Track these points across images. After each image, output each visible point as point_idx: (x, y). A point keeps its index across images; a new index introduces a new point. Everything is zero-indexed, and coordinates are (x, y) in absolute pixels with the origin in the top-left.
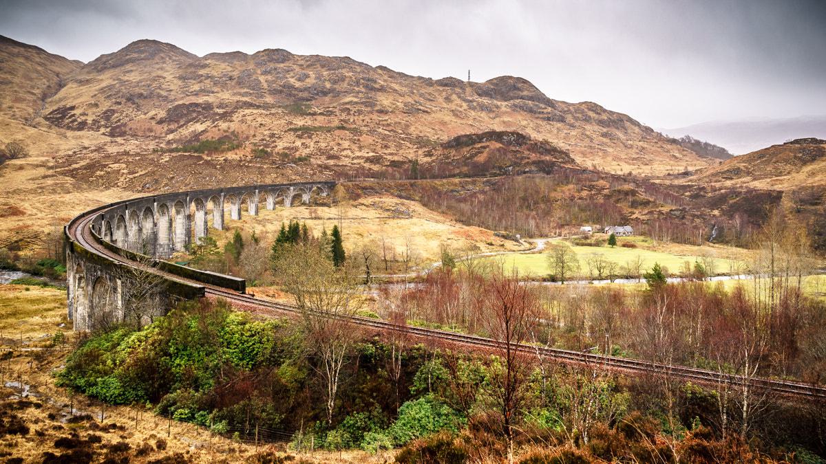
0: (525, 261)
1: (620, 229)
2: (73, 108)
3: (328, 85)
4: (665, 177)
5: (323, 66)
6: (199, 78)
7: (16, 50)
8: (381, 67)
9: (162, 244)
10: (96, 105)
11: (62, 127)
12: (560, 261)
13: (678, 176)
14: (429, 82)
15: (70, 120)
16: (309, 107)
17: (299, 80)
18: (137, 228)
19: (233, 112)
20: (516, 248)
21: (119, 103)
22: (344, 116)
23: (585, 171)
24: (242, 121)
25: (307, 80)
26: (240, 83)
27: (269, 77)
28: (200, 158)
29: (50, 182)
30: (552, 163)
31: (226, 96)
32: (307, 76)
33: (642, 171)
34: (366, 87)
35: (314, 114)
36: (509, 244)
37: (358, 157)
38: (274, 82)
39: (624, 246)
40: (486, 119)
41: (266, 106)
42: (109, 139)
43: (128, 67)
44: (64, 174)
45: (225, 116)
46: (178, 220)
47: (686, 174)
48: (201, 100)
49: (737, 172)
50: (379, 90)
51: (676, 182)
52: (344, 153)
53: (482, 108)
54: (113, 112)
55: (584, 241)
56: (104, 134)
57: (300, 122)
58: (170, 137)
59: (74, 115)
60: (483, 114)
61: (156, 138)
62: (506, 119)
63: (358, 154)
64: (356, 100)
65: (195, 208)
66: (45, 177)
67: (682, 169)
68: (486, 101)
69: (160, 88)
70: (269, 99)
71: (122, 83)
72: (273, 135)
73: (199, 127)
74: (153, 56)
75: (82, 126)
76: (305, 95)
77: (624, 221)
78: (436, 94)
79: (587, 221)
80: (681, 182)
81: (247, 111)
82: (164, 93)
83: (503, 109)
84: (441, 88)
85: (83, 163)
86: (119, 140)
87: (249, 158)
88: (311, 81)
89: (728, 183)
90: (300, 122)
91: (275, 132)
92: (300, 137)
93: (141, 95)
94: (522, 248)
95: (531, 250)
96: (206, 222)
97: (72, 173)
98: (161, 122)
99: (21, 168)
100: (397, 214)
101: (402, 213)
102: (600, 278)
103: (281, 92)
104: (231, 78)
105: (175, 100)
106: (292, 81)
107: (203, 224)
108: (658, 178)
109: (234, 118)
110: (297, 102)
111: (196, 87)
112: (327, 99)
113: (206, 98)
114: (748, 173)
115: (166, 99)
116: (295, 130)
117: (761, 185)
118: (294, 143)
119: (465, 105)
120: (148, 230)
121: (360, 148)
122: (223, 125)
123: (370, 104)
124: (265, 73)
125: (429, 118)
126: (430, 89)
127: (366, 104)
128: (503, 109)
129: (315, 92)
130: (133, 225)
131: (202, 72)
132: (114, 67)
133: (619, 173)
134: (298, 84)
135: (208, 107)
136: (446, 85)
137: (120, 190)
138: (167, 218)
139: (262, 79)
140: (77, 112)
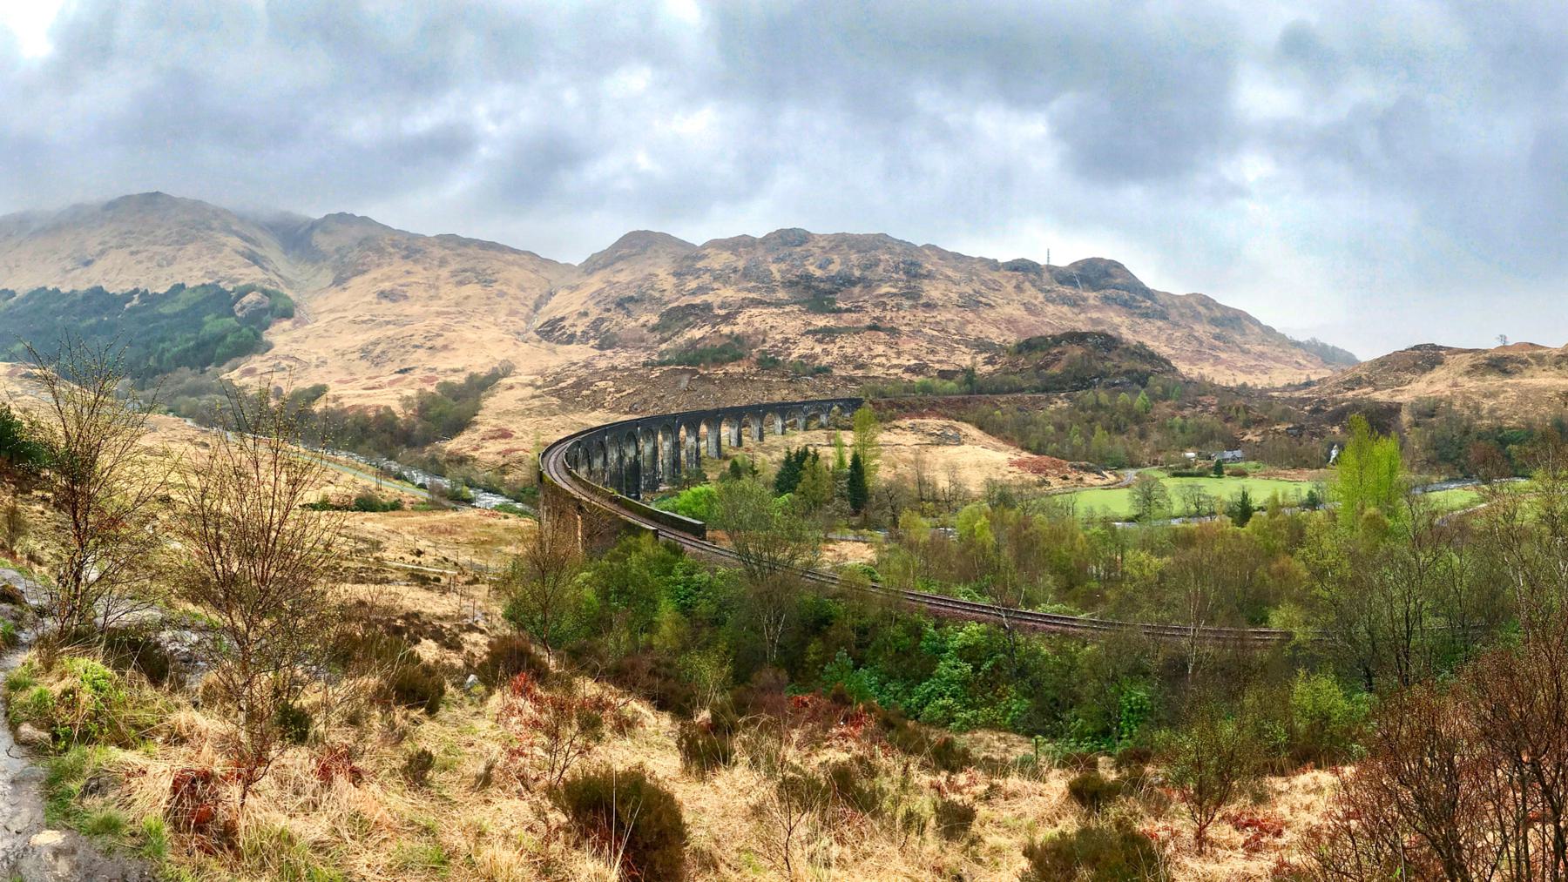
0: (1103, 499)
1: (1229, 455)
2: (563, 319)
3: (857, 273)
4: (1284, 389)
5: (851, 247)
6: (697, 274)
7: (511, 257)
8: (929, 247)
10: (586, 314)
12: (1148, 498)
13: (1298, 388)
14: (994, 265)
16: (833, 302)
17: (820, 267)
19: (738, 313)
20: (1099, 482)
21: (608, 310)
22: (877, 313)
23: (1190, 382)
24: (748, 324)
25: (831, 267)
26: (746, 275)
27: (783, 266)
28: (695, 372)
29: (537, 402)
30: (1145, 369)
31: (729, 293)
32: (831, 262)
33: (1258, 381)
34: (907, 273)
35: (839, 311)
36: (1089, 478)
37: (895, 366)
38: (788, 271)
39: (1231, 474)
40: (1070, 315)
41: (779, 304)
42: (597, 352)
43: (619, 266)
44: (550, 394)
45: (727, 319)
47: (1308, 384)
48: (698, 300)
49: (1357, 382)
50: (925, 277)
51: (1297, 394)
52: (877, 361)
53: (1065, 300)
54: (603, 320)
55: (1183, 471)
57: (820, 322)
58: (664, 346)
60: (1065, 309)
61: (647, 349)
62: (1095, 315)
63: (895, 362)
64: (894, 290)
66: (534, 397)
67: (1303, 379)
68: (1068, 291)
69: (652, 288)
70: (782, 294)
71: (611, 284)
72: (786, 340)
73: (697, 334)
74: (644, 249)
75: (571, 339)
76: (827, 286)
77: (1233, 444)
78: (1003, 282)
79: (1189, 446)
80: (1303, 394)
81: (755, 311)
82: (657, 295)
83: (1091, 302)
84: (1009, 274)
85: (570, 381)
86: (609, 353)
87: (754, 370)
88: (835, 268)
89: (1350, 394)
90: (820, 322)
92: (820, 341)
93: (631, 299)
94: (1106, 482)
95: (1115, 485)
97: (558, 393)
98: (654, 329)
99: (511, 387)
100: (942, 439)
101: (948, 437)
102: (1198, 514)
103: (797, 283)
104: (735, 271)
105: (669, 302)
106: (811, 269)
108: (1276, 390)
109: (739, 320)
110: (816, 295)
111: (692, 284)
112: (857, 290)
113: (704, 297)
114: (1370, 383)
115: (658, 301)
116: (815, 332)
117: (1382, 396)
119: (1041, 296)
121: (899, 354)
122: (726, 330)
123: (913, 295)
124: (778, 260)
125: (993, 314)
126: (996, 275)
127: (908, 296)
128: (1091, 302)
131: (700, 265)
132: (605, 267)
133: (1232, 384)
134: (818, 273)
135: (707, 307)
136: (1016, 269)
139: (774, 268)
140: (566, 323)
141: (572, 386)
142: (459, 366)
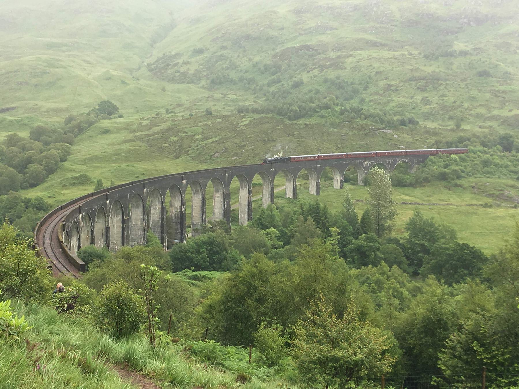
2: (178, 55)
11: (163, 79)
15: (172, 70)
18: (160, 207)
37: (494, 118)
42: (207, 94)
46: (216, 199)
56: (203, 87)
63: (496, 112)
65: (212, 189)
91: (393, 83)
96: (249, 202)
99: (106, 131)
107: (247, 204)
118: (412, 97)
120: (177, 208)
129: (465, 20)
130: (157, 203)
137: (189, 159)
138: (201, 197)
141: (163, 132)
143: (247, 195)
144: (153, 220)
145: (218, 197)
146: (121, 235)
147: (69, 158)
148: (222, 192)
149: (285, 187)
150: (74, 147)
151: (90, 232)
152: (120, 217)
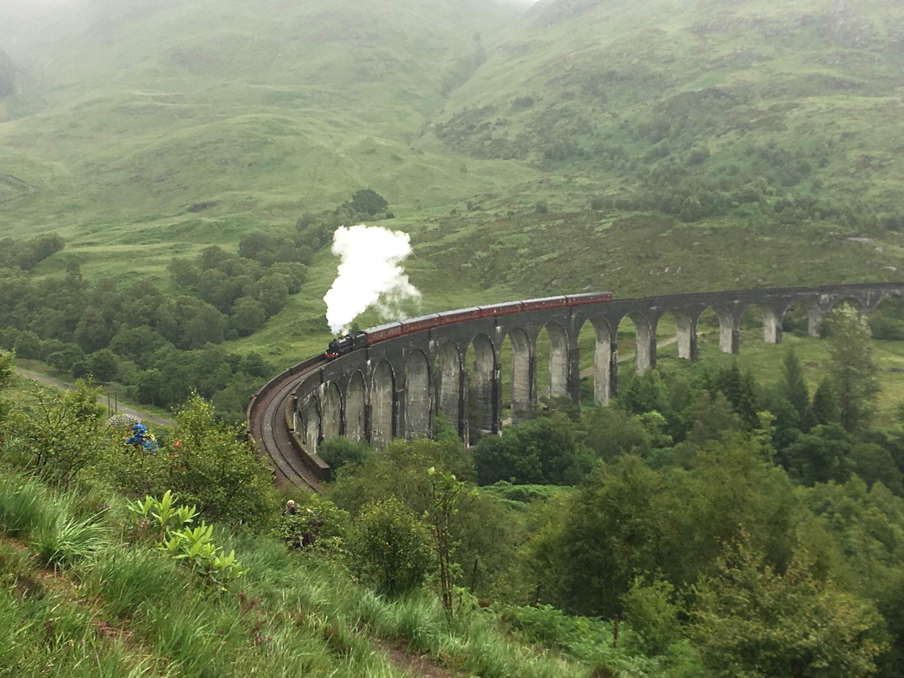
9: (518, 401)
11: (464, 152)
15: (480, 136)
42: (537, 176)
46: (555, 359)
56: (531, 165)
59: (486, 126)
65: (548, 342)
72: (865, 162)
91: (875, 153)
96: (612, 365)
107: (608, 367)
120: (485, 374)
137: (508, 289)
138: (527, 355)
141: (461, 242)
142: (295, 198)
143: (609, 352)
144: (446, 395)
145: (558, 356)
146: (389, 419)
147: (303, 287)
148: (564, 348)
149: (673, 340)
150: (313, 270)
151: (338, 415)
152: (389, 389)
